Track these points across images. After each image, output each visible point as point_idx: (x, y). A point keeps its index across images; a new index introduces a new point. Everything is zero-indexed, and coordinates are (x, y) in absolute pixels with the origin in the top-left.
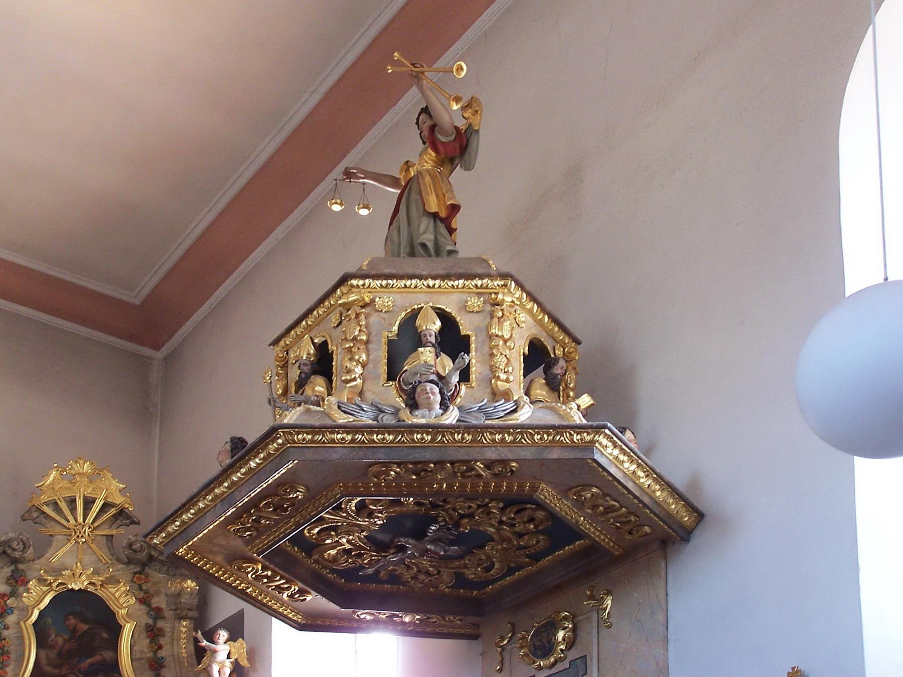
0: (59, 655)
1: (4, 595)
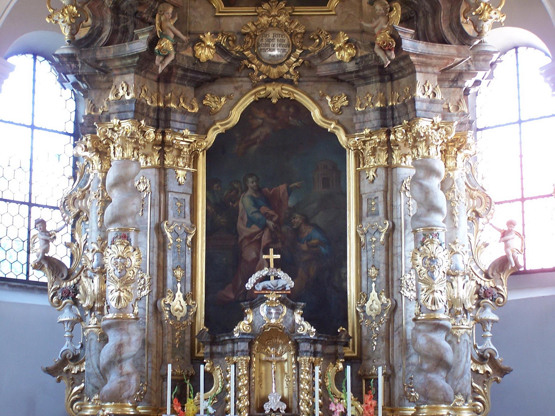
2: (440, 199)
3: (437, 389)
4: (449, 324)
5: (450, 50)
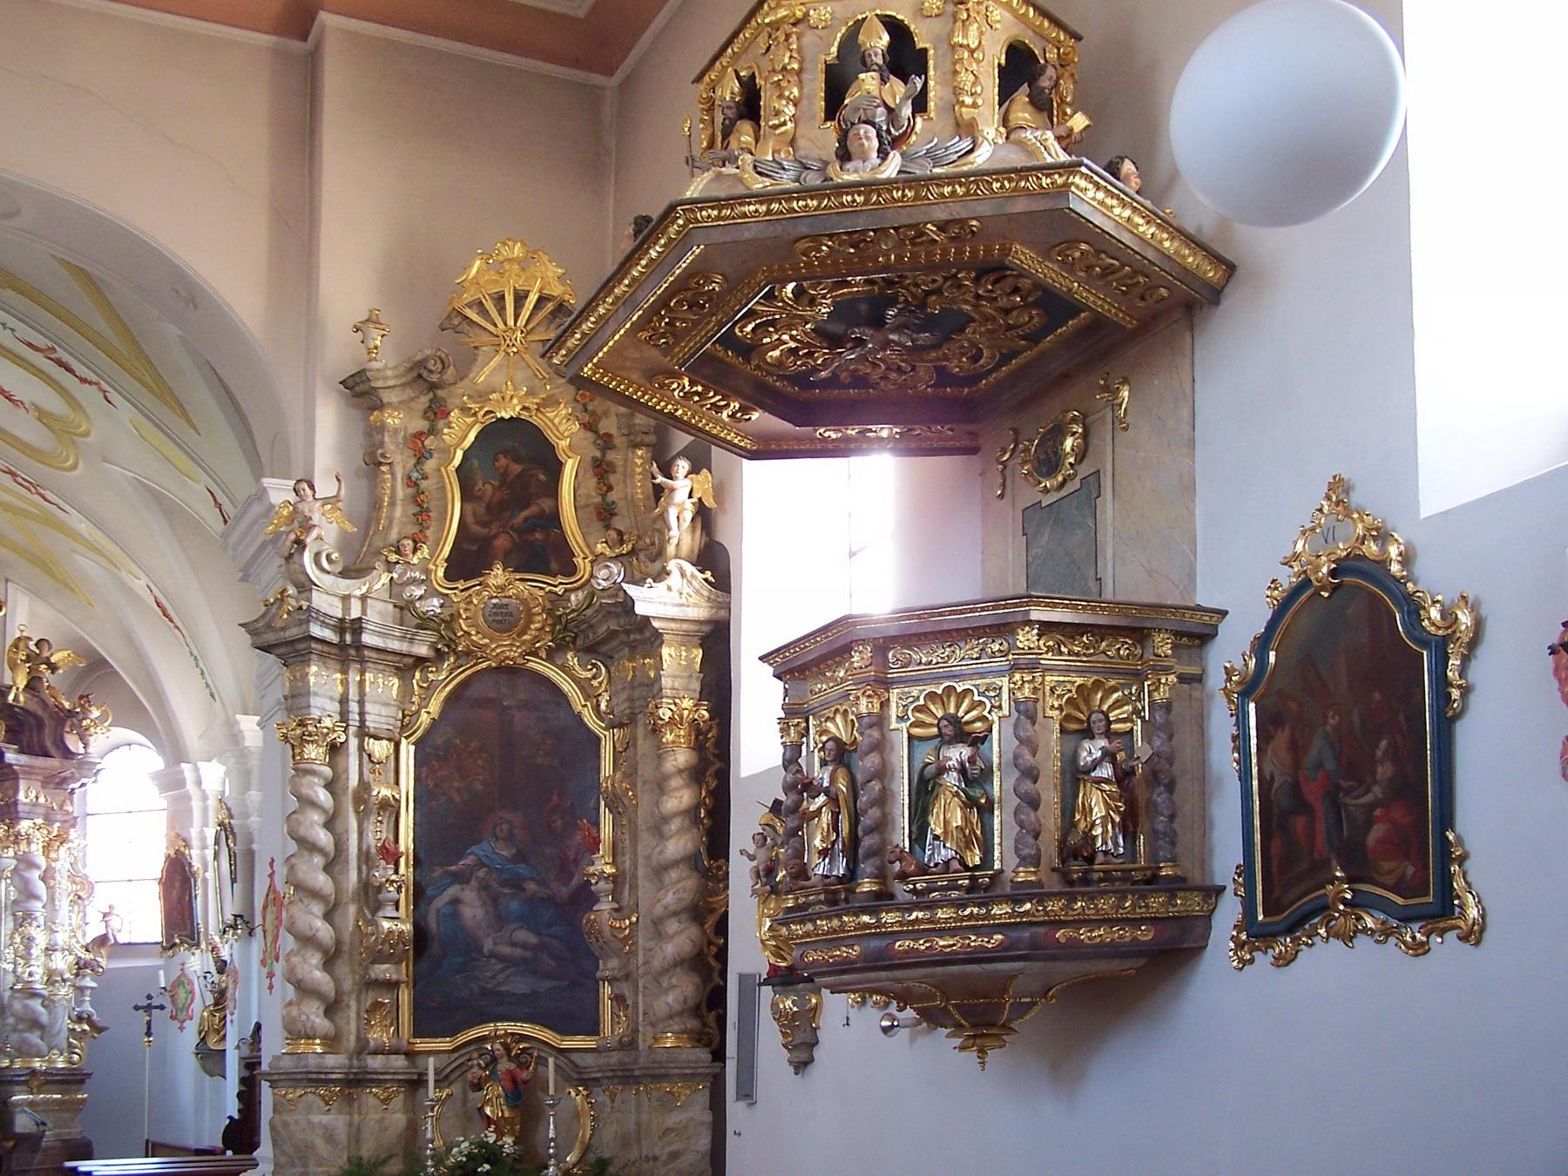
0: (489, 508)
1: (421, 433)
2: (41, 889)
3: (31, 1045)
4: (45, 993)
5: (54, 763)
